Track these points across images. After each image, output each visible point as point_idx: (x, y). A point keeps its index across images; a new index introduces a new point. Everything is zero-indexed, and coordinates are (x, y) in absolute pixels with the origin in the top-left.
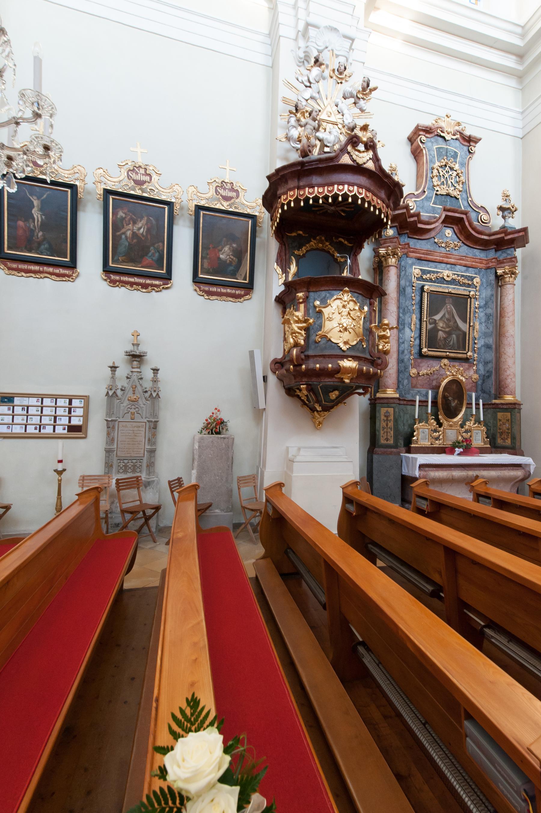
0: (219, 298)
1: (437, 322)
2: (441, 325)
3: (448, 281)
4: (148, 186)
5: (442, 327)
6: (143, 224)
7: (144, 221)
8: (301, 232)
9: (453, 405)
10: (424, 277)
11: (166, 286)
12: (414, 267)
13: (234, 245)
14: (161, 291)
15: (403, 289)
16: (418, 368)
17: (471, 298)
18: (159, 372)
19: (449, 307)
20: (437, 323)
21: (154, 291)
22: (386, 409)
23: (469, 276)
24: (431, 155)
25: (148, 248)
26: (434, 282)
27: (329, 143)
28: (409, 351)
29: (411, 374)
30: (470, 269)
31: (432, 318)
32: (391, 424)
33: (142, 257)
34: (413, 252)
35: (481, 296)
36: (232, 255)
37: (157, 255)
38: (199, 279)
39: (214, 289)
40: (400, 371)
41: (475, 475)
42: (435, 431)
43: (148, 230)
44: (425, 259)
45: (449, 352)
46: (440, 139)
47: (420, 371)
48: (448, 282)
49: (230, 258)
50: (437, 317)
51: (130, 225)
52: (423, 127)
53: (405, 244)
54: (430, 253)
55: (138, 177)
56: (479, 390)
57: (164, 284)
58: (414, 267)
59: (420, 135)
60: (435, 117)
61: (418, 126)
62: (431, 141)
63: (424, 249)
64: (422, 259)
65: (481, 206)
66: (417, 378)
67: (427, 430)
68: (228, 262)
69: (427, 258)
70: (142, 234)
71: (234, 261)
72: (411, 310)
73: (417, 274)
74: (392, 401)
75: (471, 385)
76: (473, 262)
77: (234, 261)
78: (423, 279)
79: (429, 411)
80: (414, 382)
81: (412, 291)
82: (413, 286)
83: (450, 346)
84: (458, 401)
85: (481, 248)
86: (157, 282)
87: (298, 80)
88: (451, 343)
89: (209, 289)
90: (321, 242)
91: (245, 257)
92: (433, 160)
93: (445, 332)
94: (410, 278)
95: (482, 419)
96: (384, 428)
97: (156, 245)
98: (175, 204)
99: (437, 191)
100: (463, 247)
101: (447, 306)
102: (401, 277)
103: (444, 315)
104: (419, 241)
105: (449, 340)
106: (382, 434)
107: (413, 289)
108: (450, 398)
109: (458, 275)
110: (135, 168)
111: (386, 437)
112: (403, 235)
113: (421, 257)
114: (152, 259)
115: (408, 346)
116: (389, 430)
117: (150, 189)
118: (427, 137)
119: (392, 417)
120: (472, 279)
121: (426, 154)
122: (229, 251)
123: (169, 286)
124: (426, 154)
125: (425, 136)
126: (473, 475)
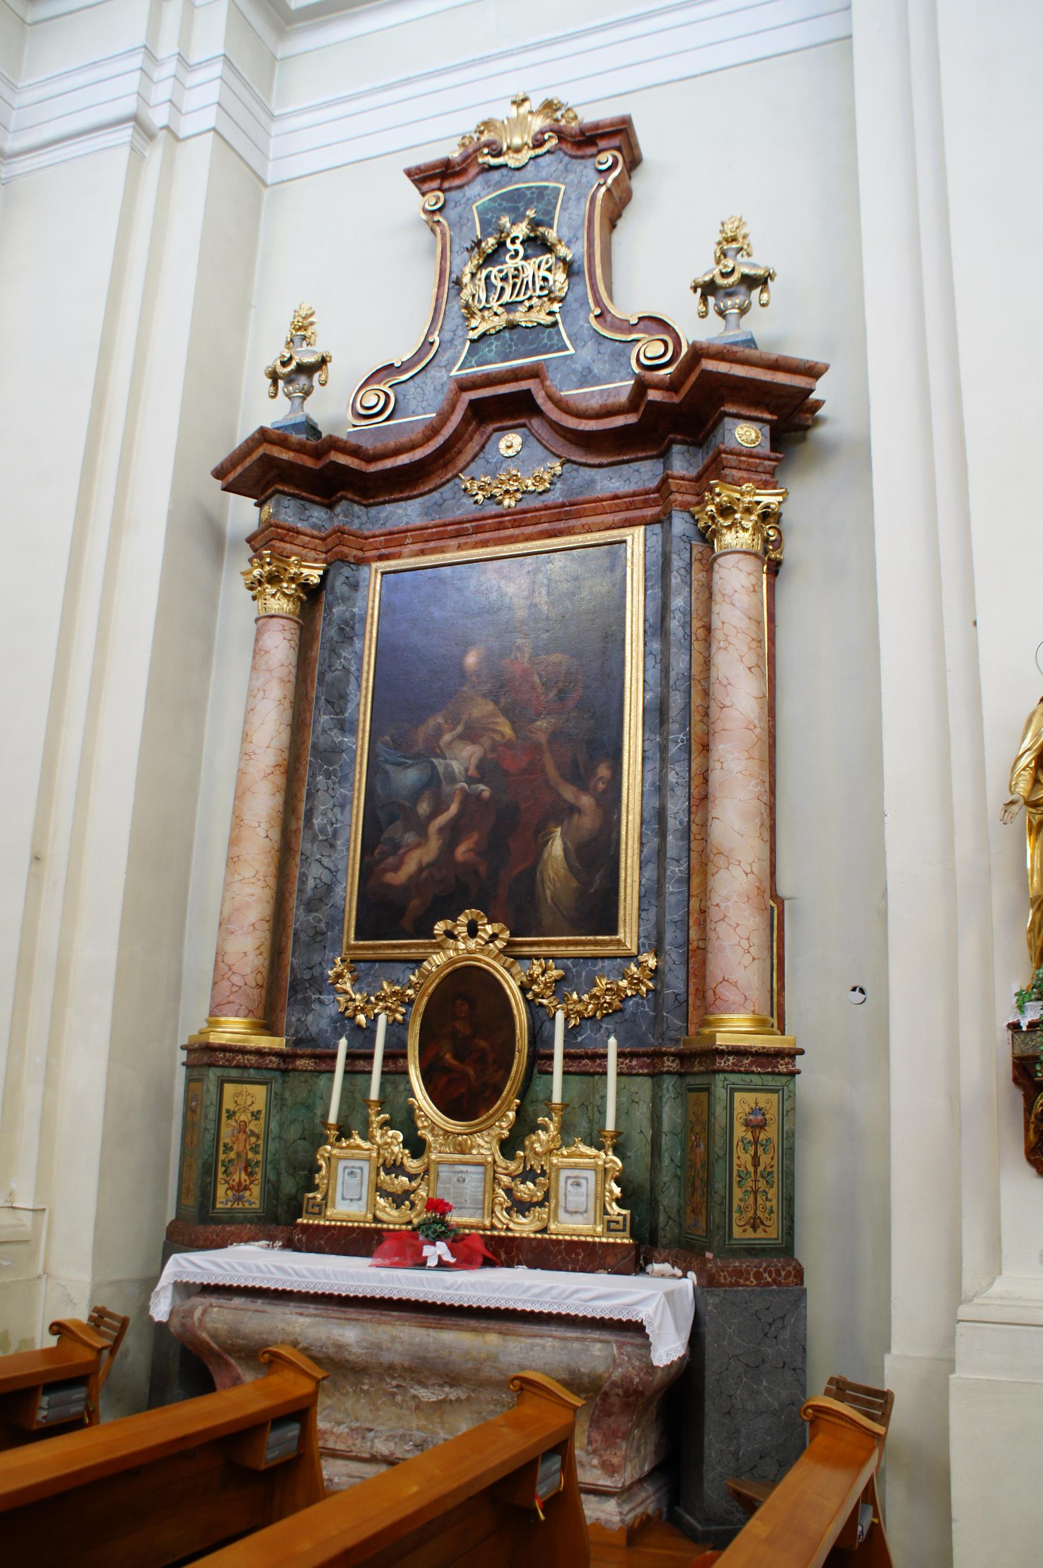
42: (395, 1168)
65: (640, 319)
67: (366, 1166)
79: (374, 1094)
95: (610, 1126)
118: (443, 191)
125: (440, 189)
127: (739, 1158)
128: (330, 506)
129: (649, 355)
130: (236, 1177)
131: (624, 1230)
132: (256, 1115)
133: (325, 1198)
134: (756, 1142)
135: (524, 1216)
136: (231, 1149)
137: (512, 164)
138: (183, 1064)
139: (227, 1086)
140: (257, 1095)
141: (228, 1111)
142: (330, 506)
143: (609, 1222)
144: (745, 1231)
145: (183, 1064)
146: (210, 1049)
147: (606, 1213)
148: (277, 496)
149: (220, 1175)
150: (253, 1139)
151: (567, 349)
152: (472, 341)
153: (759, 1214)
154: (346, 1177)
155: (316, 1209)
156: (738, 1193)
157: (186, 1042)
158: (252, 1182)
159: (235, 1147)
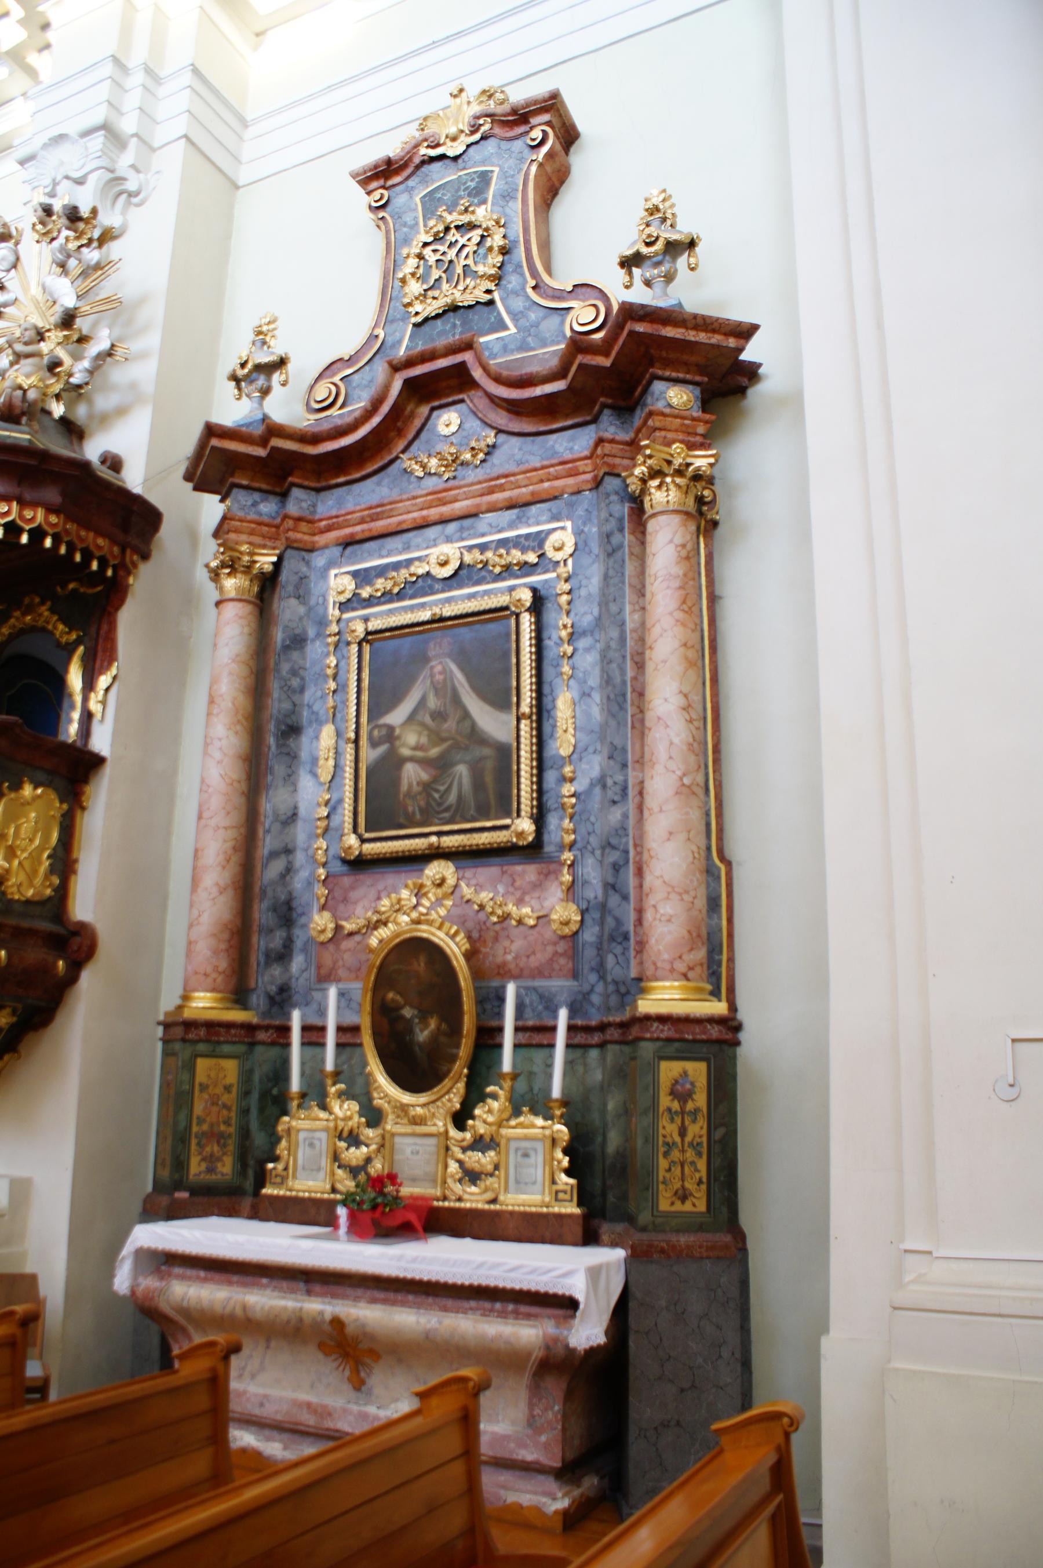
1: (397, 732)
2: (411, 738)
3: (445, 579)
5: (415, 748)
9: (422, 1036)
10: (365, 593)
17: (518, 615)
19: (439, 668)
20: (398, 738)
23: (528, 536)
26: (400, 596)
30: (534, 509)
31: (382, 721)
34: (329, 529)
35: (583, 592)
41: (328, 1317)
42: (354, 1139)
44: (367, 535)
45: (439, 834)
46: (436, 166)
48: (455, 579)
50: (396, 717)
52: (365, 173)
54: (382, 512)
56: (586, 968)
64: (358, 538)
65: (575, 286)
66: (338, 946)
69: (370, 530)
72: (322, 712)
75: (550, 949)
76: (542, 481)
78: (365, 600)
79: (330, 1066)
83: (447, 810)
84: (442, 1019)
85: (569, 422)
88: (452, 798)
93: (425, 763)
94: (321, 610)
100: (506, 447)
101: (432, 668)
103: (422, 702)
105: (442, 788)
107: (328, 644)
108: (408, 1012)
109: (483, 548)
113: (352, 535)
120: (538, 540)
125: (383, 187)
126: (321, 1313)
127: (664, 1128)
129: (581, 322)
130: (208, 1149)
131: (571, 1200)
132: (228, 1089)
133: (286, 1169)
134: (683, 1112)
135: (475, 1185)
136: (204, 1121)
137: (451, 153)
140: (230, 1069)
141: (201, 1085)
143: (557, 1192)
144: (672, 1204)
145: (161, 1039)
146: (190, 1025)
147: (554, 1182)
149: (193, 1147)
150: (225, 1112)
151: (506, 328)
152: (415, 325)
153: (687, 1185)
155: (279, 1180)
156: (663, 1163)
158: (224, 1154)
159: (208, 1119)
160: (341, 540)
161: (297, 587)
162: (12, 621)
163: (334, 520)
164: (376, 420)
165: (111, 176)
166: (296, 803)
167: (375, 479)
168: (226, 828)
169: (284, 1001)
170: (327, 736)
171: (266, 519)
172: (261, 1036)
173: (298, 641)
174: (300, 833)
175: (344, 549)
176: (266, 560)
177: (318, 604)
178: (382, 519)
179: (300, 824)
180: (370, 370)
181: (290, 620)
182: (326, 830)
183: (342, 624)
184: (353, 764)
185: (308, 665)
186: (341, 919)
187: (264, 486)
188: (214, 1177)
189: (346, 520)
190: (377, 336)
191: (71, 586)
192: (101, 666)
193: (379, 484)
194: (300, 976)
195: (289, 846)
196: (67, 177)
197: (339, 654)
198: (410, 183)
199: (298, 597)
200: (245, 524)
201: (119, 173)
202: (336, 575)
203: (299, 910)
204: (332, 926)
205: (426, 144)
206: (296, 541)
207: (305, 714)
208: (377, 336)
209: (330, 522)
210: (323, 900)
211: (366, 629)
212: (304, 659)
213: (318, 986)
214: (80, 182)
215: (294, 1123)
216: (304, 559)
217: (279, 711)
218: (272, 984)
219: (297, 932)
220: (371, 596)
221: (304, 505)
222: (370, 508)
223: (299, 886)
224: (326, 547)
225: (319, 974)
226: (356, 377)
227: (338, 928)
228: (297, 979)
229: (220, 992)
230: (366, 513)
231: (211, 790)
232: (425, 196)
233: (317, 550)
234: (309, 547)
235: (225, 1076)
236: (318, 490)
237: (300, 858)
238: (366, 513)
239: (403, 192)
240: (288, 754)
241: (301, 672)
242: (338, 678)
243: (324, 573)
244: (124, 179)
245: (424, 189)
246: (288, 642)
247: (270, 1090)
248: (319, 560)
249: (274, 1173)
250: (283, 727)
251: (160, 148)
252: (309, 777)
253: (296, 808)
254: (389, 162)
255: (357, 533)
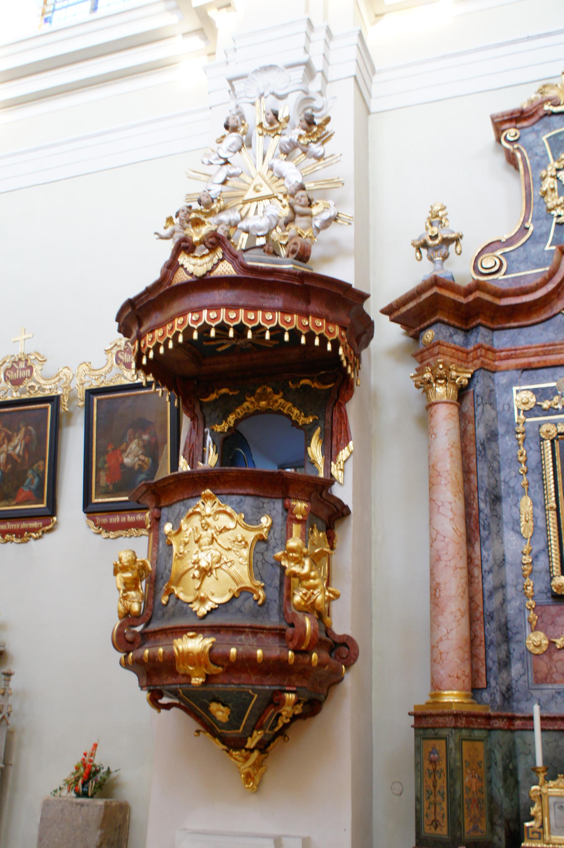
0: (123, 532)
4: (28, 382)
6: (19, 440)
7: (21, 435)
8: (224, 391)
11: (47, 528)
12: (515, 389)
13: (146, 437)
14: (40, 537)
15: (482, 444)
16: (551, 628)
18: (12, 678)
21: (32, 539)
22: (432, 742)
24: (536, 154)
25: (26, 472)
27: (260, 230)
28: (520, 587)
29: (531, 648)
32: (442, 782)
33: (17, 488)
34: (508, 358)
36: (142, 454)
37: (36, 480)
38: (93, 506)
39: (115, 519)
40: (488, 643)
43: (27, 447)
44: (542, 364)
46: (554, 119)
47: (558, 637)
49: (140, 460)
51: (5, 446)
52: (503, 116)
53: (475, 349)
54: (554, 350)
55: (15, 376)
57: (44, 525)
58: (515, 389)
59: (503, 131)
60: (538, 86)
61: (493, 119)
62: (533, 131)
63: (534, 345)
64: (534, 366)
66: (551, 657)
68: (137, 467)
69: (545, 361)
70: (18, 455)
71: (146, 464)
72: (517, 487)
73: (524, 404)
74: (441, 720)
77: (146, 464)
78: (545, 410)
80: (543, 666)
81: (515, 443)
82: (518, 433)
86: (35, 524)
87: (203, 163)
89: (109, 520)
90: (264, 396)
91: (164, 453)
92: (544, 162)
94: (508, 415)
96: (429, 793)
97: (35, 467)
98: (61, 397)
99: (559, 216)
102: (477, 418)
104: (524, 330)
106: (425, 810)
107: (518, 439)
110: (14, 364)
111: (433, 818)
112: (474, 330)
113: (530, 364)
114: (30, 488)
115: (517, 577)
116: (439, 798)
117: (29, 387)
118: (519, 129)
119: (442, 765)
121: (523, 158)
122: (137, 449)
123: (50, 526)
124: (523, 158)
125: (515, 128)
128: (467, 331)
138: (412, 726)
139: (464, 742)
142: (467, 331)
145: (412, 726)
148: (439, 325)
154: (557, 810)
157: (412, 710)
160: (519, 367)
161: (490, 397)
162: (246, 404)
163: (513, 352)
164: (551, 286)
165: (304, 96)
166: (504, 551)
167: (541, 326)
168: (461, 568)
169: (509, 697)
170: (526, 504)
171: (457, 346)
172: (497, 724)
173: (493, 436)
174: (510, 575)
175: (522, 372)
176: (463, 378)
177: (504, 410)
178: (552, 354)
179: (508, 568)
180: (524, 251)
181: (488, 420)
182: (532, 572)
183: (527, 426)
184: (556, 526)
185: (501, 453)
186: (551, 637)
187: (457, 324)
188: (477, 834)
189: (523, 353)
190: (527, 229)
191: (303, 382)
192: (338, 443)
193: (545, 329)
194: (519, 679)
195: (503, 584)
196: (273, 94)
197: (526, 446)
198: (536, 127)
199: (491, 404)
200: (449, 349)
201: (311, 95)
202: (517, 392)
203: (514, 630)
204: (545, 642)
205: (549, 103)
206: (487, 364)
207: (503, 487)
208: (527, 229)
209: (509, 353)
210: (535, 623)
211: (557, 431)
212: (498, 448)
213: (536, 687)
214: (280, 98)
215: (544, 790)
216: (490, 377)
217: (489, 485)
218: (503, 684)
219: (513, 646)
220: (550, 407)
221: (487, 339)
222: (544, 346)
223: (512, 612)
224: (507, 370)
225: (536, 677)
226: (513, 254)
227: (552, 643)
228: (517, 681)
229: (467, 690)
230: (540, 349)
231: (446, 540)
232: (550, 137)
233: (500, 371)
234: (493, 370)
235: (477, 755)
236: (493, 330)
237: (510, 591)
238: (540, 349)
239: (531, 132)
240: (496, 516)
241: (497, 457)
242: (527, 463)
243: (508, 388)
244: (313, 99)
245: (548, 133)
246: (489, 436)
247: (508, 765)
248: (501, 379)
249: (530, 829)
250: (492, 497)
251: (332, 82)
252: (512, 533)
253: (504, 555)
254: (522, 112)
255: (533, 363)
